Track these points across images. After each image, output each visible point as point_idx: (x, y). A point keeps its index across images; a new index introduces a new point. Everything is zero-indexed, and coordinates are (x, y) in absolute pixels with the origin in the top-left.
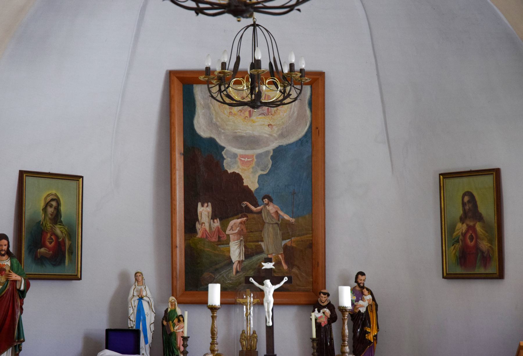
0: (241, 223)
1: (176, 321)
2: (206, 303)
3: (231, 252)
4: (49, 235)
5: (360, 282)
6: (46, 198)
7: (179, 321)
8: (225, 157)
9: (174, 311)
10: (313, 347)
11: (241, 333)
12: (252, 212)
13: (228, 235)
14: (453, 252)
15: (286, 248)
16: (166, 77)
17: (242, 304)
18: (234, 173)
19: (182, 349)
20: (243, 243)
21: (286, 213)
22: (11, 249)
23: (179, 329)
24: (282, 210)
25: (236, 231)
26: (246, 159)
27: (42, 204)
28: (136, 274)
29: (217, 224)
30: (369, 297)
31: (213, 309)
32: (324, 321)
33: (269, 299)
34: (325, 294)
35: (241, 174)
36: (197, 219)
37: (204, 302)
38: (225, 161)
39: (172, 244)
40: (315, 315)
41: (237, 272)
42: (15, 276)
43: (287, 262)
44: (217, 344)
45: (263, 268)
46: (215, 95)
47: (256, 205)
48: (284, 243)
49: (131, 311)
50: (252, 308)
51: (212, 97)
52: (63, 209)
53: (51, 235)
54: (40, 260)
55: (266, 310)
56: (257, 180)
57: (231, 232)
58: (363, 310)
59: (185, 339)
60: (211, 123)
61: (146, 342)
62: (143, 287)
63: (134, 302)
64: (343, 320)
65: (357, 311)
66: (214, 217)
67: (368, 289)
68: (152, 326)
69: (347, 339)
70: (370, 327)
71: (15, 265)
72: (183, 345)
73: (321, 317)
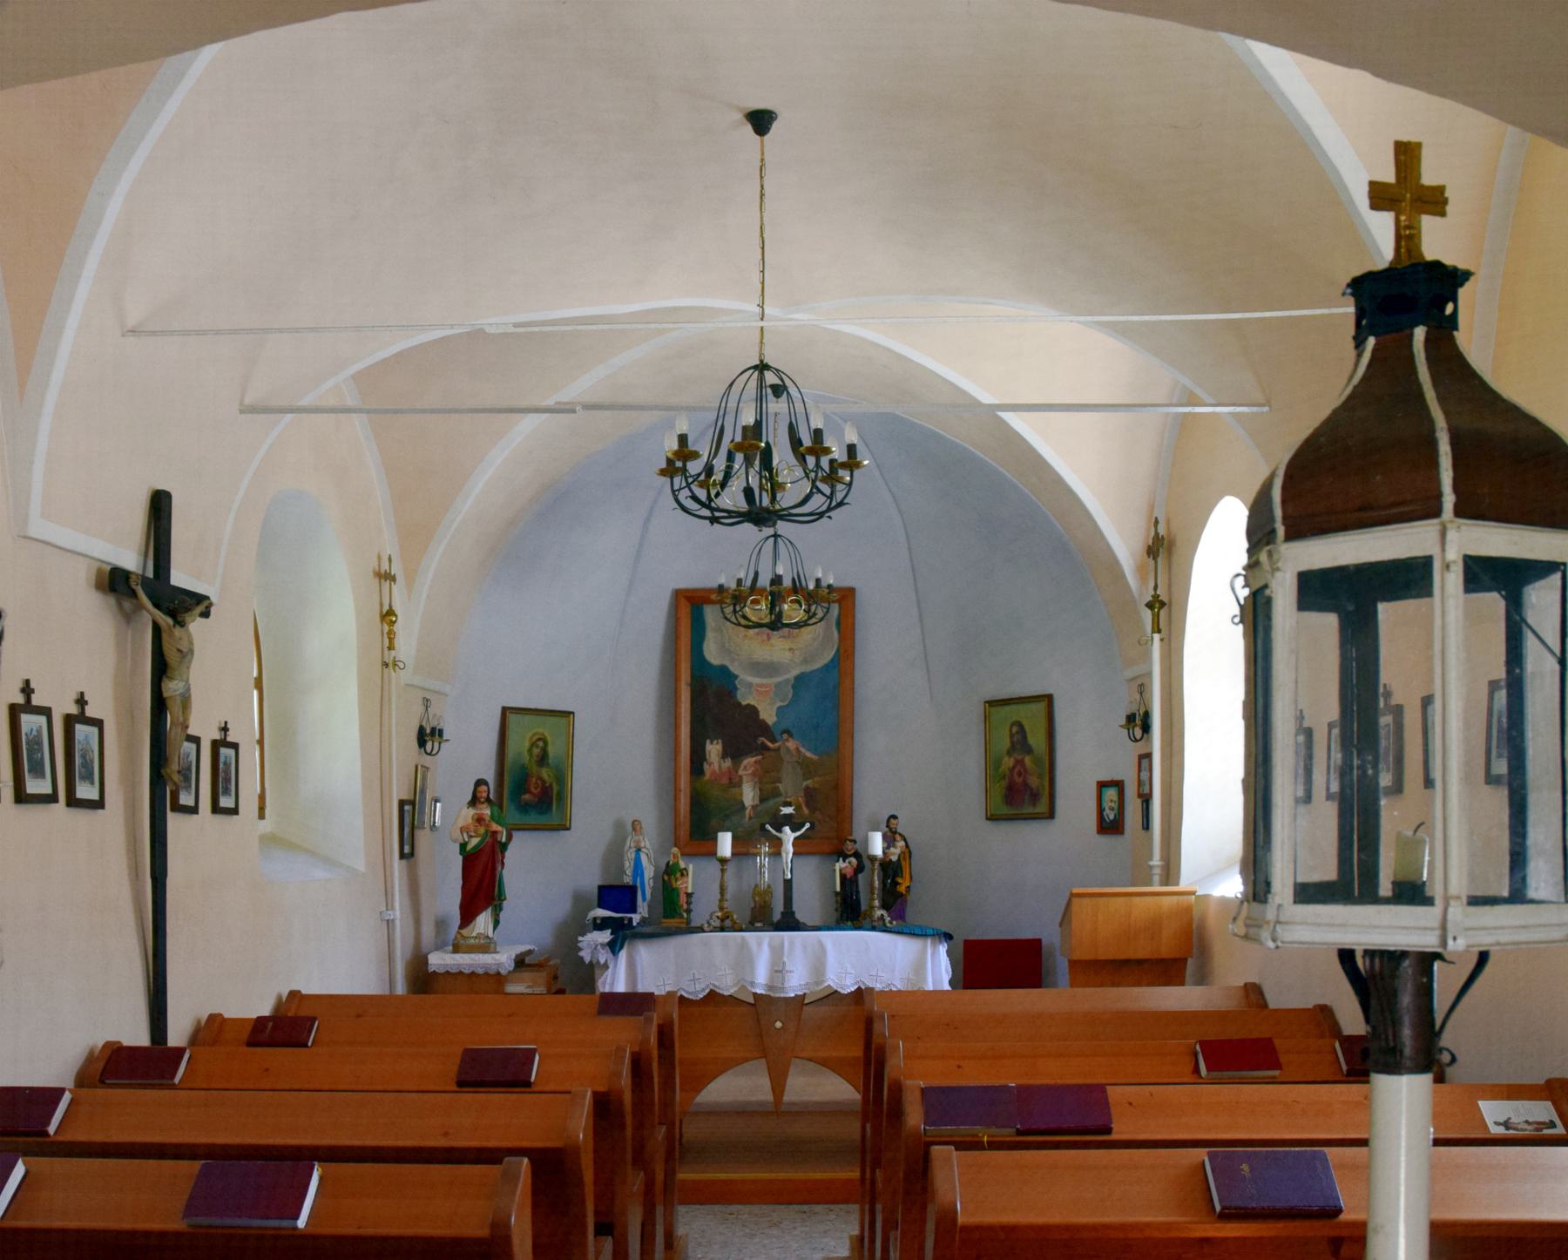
0: (755, 762)
1: (678, 874)
2: (716, 854)
3: (744, 795)
4: (534, 779)
5: (892, 826)
6: (531, 738)
7: (682, 875)
8: (738, 686)
9: (678, 863)
10: (837, 902)
11: (753, 887)
12: (768, 749)
13: (741, 777)
14: (999, 789)
15: (807, 789)
16: (672, 597)
17: (755, 855)
18: (748, 705)
19: (685, 906)
20: (758, 785)
21: (808, 750)
22: (491, 797)
23: (681, 884)
24: (803, 746)
25: (750, 771)
26: (763, 689)
27: (527, 744)
28: (634, 822)
29: (728, 763)
30: (902, 843)
31: (723, 861)
32: (849, 872)
33: (789, 848)
34: (851, 841)
35: (756, 705)
36: (705, 759)
37: (712, 853)
38: (738, 692)
39: (676, 787)
40: (840, 865)
41: (750, 818)
42: (495, 827)
43: (807, 805)
44: (726, 900)
45: (782, 813)
46: (729, 616)
47: (773, 741)
48: (805, 783)
49: (627, 864)
50: (767, 859)
51: (726, 618)
52: (550, 749)
53: (537, 780)
54: (524, 808)
55: (784, 861)
56: (775, 713)
57: (745, 772)
58: (894, 858)
59: (689, 895)
60: (724, 649)
61: (644, 899)
62: (641, 837)
63: (631, 855)
64: (873, 871)
65: (887, 860)
66: (724, 755)
67: (900, 835)
68: (651, 881)
69: (876, 892)
70: (902, 877)
71: (496, 814)
72: (687, 903)
73: (846, 867)
